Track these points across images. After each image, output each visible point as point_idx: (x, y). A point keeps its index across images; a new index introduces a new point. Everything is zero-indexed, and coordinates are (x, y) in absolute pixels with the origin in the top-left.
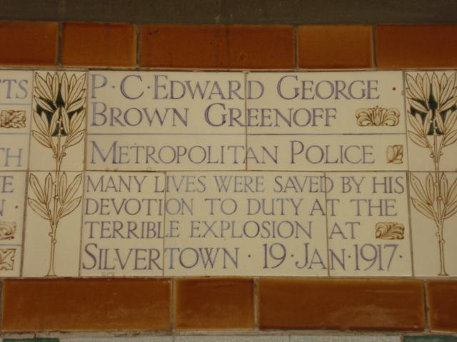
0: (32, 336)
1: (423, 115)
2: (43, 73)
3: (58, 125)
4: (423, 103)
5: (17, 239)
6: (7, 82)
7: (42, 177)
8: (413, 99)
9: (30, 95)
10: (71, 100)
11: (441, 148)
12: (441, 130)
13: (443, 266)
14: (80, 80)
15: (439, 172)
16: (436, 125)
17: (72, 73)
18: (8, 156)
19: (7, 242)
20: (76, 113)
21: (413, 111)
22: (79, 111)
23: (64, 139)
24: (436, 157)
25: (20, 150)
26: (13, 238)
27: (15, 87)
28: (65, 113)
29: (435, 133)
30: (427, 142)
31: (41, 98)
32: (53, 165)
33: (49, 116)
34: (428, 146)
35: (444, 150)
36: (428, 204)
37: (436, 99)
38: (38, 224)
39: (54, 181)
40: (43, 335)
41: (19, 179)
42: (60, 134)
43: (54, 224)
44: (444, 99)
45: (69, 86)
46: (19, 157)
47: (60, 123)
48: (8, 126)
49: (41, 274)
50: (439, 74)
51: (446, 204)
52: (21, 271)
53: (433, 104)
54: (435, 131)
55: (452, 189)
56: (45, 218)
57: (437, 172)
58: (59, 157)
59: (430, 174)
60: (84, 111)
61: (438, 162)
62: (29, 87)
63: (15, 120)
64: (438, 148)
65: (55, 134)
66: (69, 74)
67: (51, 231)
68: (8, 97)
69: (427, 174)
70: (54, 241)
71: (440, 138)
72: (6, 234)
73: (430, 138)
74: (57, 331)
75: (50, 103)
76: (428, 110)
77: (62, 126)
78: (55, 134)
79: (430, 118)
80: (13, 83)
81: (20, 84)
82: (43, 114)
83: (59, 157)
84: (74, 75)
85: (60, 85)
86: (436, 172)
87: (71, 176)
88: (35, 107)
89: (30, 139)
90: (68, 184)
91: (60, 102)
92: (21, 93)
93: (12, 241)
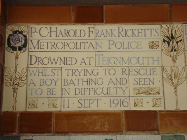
0: (173, 135)
2: (164, 26)
3: (172, 47)
5: (161, 94)
6: (150, 30)
7: (168, 69)
9: (160, 35)
10: (177, 36)
14: (180, 28)
17: (176, 25)
18: (153, 60)
19: (157, 95)
20: (180, 42)
22: (181, 41)
23: (175, 53)
25: (158, 58)
26: (160, 94)
27: (153, 31)
28: (175, 42)
31: (164, 36)
32: (172, 63)
33: (169, 43)
38: (169, 89)
39: (173, 70)
40: (178, 134)
41: (159, 70)
42: (174, 51)
43: (176, 88)
45: (176, 31)
46: (158, 60)
47: (173, 46)
48: (152, 48)
49: (173, 108)
52: (165, 107)
56: (172, 86)
58: (174, 60)
60: (183, 41)
62: (159, 31)
63: (155, 45)
65: (172, 51)
66: (175, 26)
67: (175, 91)
68: (151, 36)
70: (176, 95)
72: (157, 92)
74: (183, 133)
75: (168, 38)
77: (174, 47)
78: (172, 51)
80: (152, 30)
81: (155, 31)
82: (166, 42)
83: (174, 60)
84: (177, 26)
85: (172, 30)
87: (180, 68)
88: (162, 40)
89: (162, 53)
90: (180, 71)
91: (173, 37)
92: (156, 34)
93: (159, 95)
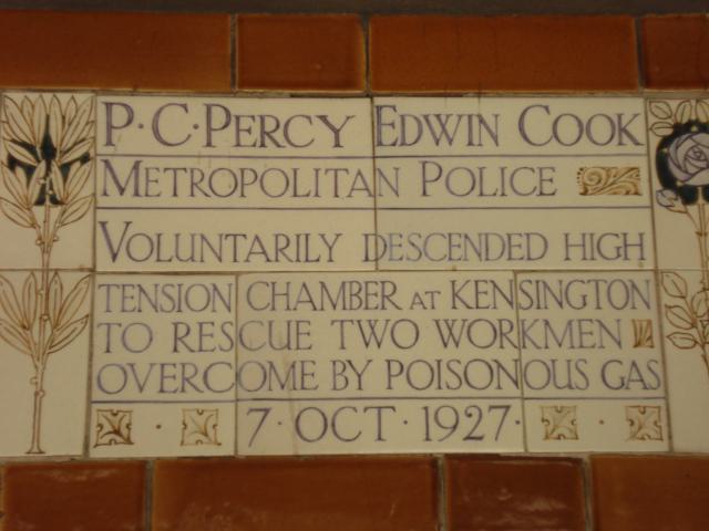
1: (30, 170)
4: (30, 148)
8: (14, 141)
11: (56, 229)
12: (59, 199)
13: (36, 437)
15: (49, 270)
16: (51, 188)
21: (13, 163)
24: (45, 244)
29: (48, 202)
30: (33, 218)
34: (33, 225)
35: (61, 232)
36: (24, 327)
37: (55, 141)
44: (68, 142)
50: (64, 97)
51: (55, 326)
53: (48, 151)
54: (48, 198)
55: (70, 299)
57: (46, 270)
59: (33, 274)
61: (49, 253)
64: (51, 228)
69: (29, 273)
71: (56, 211)
73: (39, 211)
76: (39, 161)
79: (42, 174)
86: (43, 271)
